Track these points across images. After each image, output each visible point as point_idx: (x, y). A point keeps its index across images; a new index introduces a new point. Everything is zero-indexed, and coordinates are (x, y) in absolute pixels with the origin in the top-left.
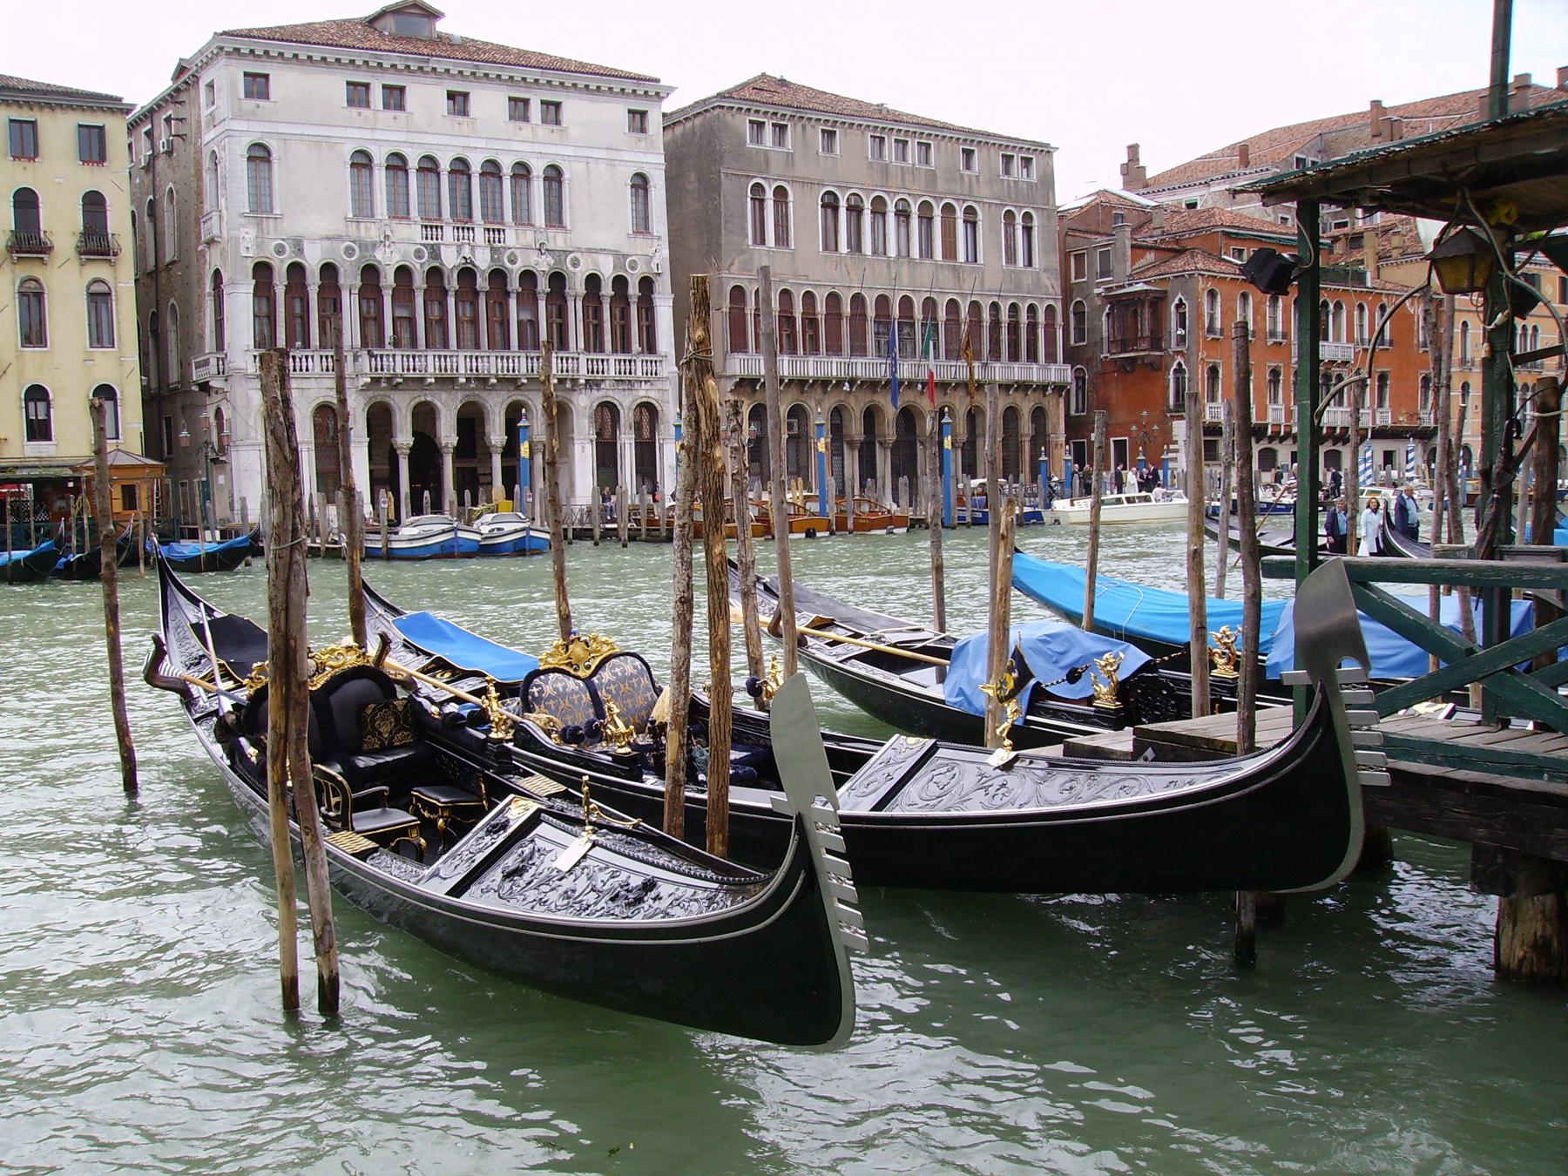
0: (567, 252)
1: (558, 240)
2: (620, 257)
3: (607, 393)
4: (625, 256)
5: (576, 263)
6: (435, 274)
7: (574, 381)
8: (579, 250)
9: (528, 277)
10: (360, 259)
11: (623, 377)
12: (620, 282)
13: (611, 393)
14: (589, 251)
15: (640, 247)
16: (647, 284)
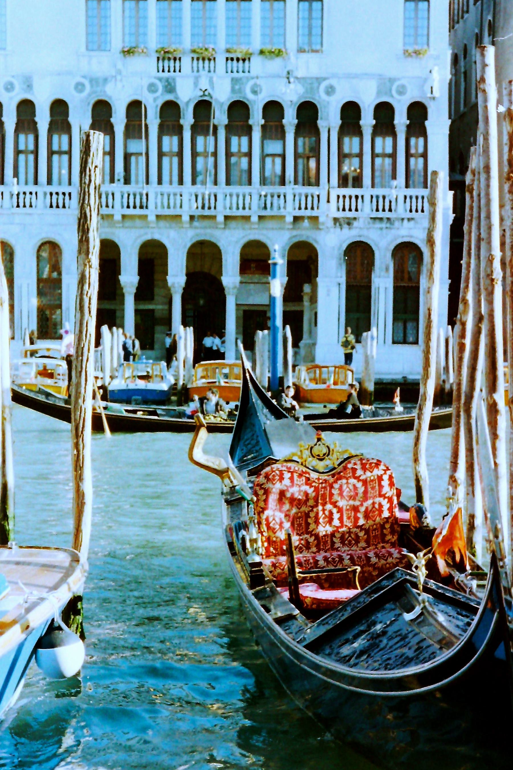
0: (319, 80)
1: (306, 66)
2: (386, 83)
3: (363, 231)
4: (392, 81)
5: (330, 90)
6: (170, 110)
7: (314, 219)
8: (335, 76)
9: (273, 109)
10: (89, 95)
11: (380, 214)
12: (384, 112)
13: (365, 232)
14: (349, 76)
15: (413, 69)
16: (418, 112)
